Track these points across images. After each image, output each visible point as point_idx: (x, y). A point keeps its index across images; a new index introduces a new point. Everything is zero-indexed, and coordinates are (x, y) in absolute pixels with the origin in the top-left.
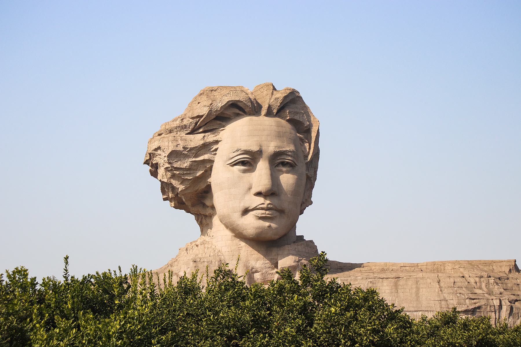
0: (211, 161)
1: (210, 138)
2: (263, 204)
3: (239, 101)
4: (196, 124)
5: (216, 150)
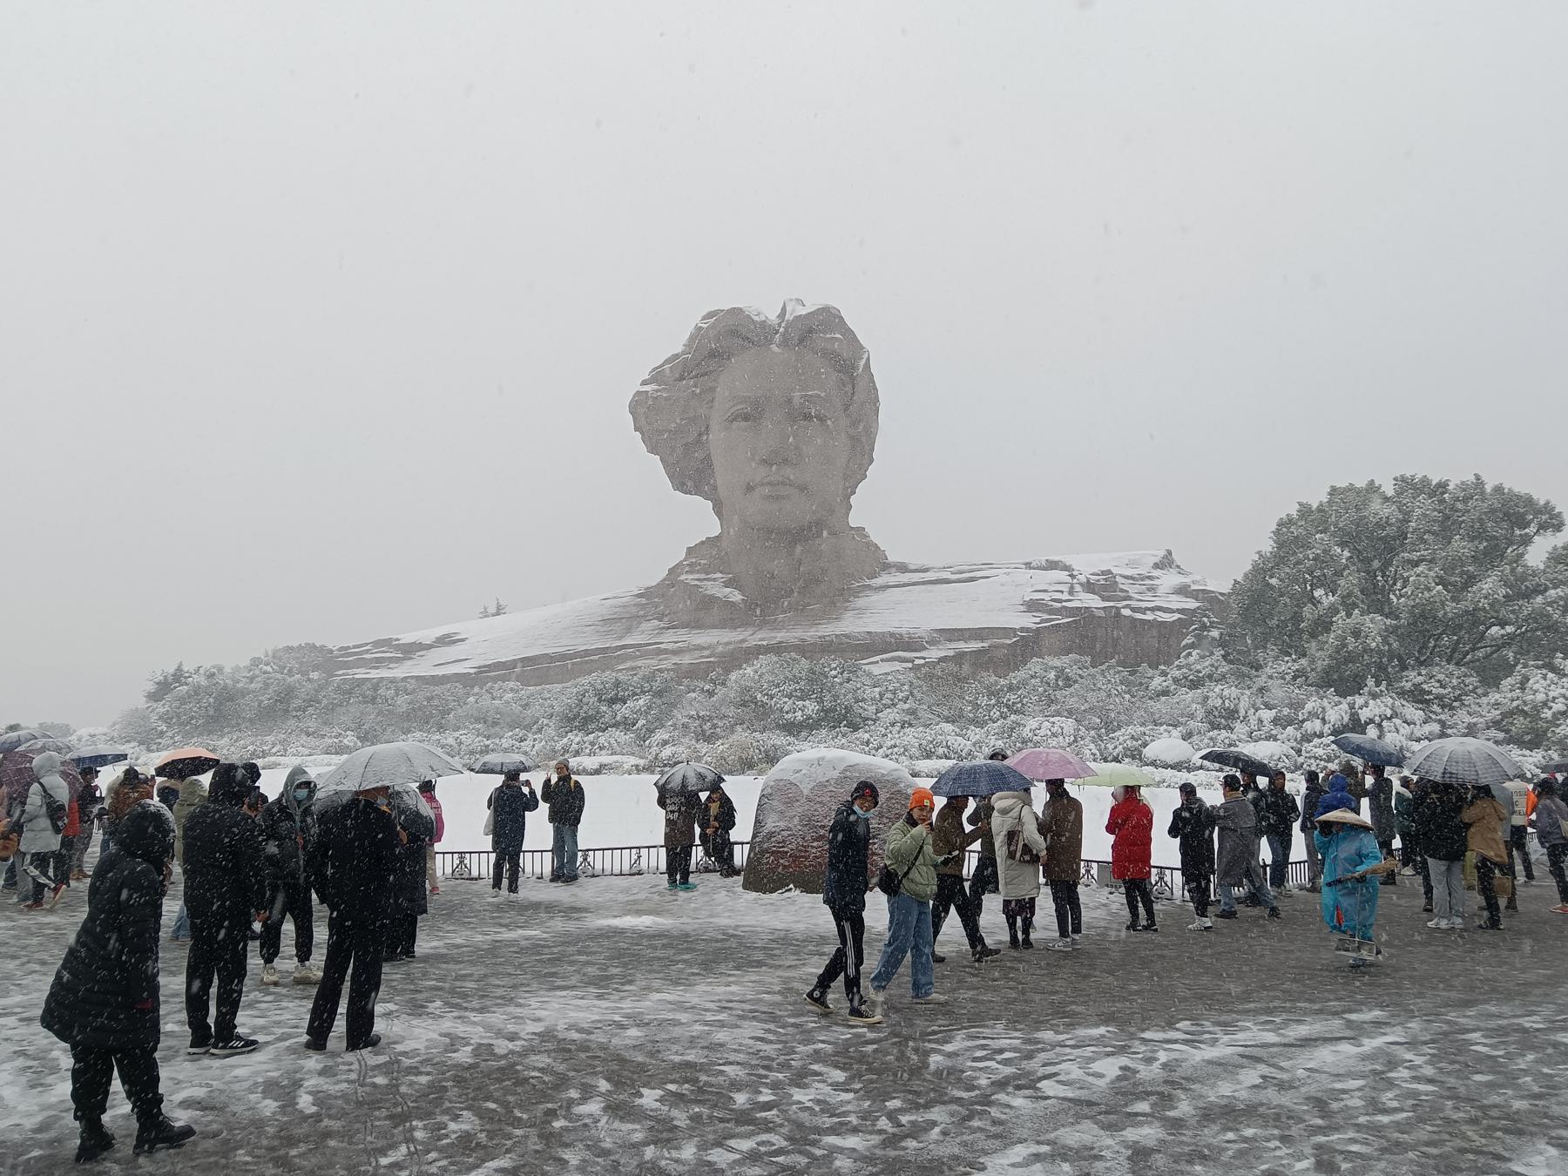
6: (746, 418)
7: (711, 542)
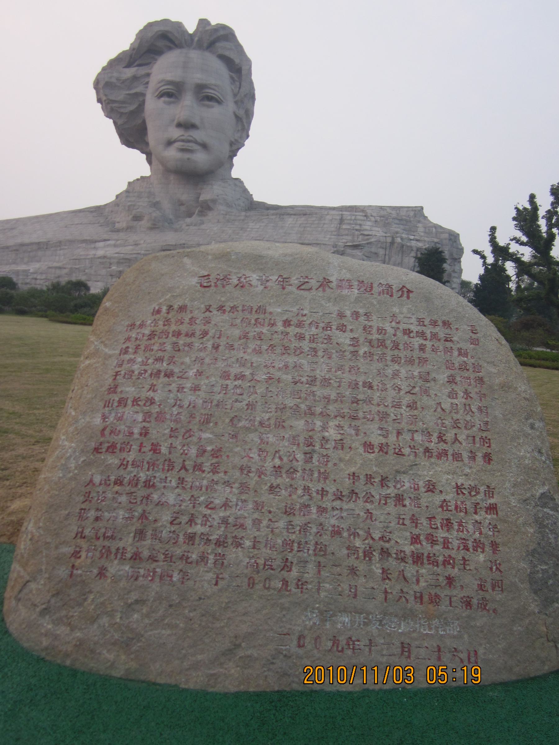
0: (143, 95)
1: (142, 71)
2: (183, 135)
5: (147, 83)
6: (169, 95)
7: (143, 178)
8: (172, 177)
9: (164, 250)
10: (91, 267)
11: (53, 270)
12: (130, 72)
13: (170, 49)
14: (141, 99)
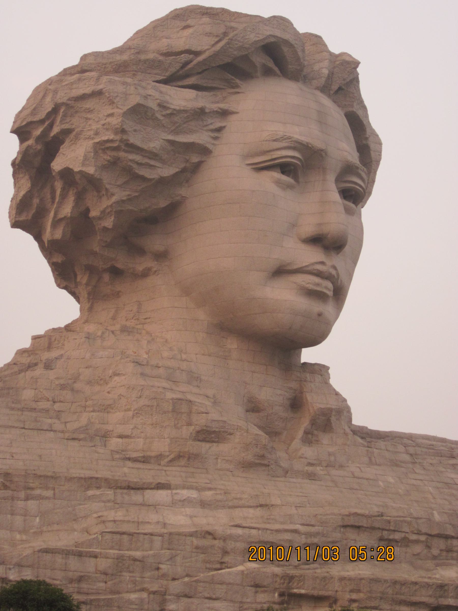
0: (205, 151)
2: (322, 263)
3: (286, 42)
4: (187, 63)
5: (219, 130)
6: (285, 168)
8: (232, 344)
9: (308, 525)
10: (172, 558)
11: (59, 559)
12: (181, 98)
13: (268, 72)
14: (195, 159)
